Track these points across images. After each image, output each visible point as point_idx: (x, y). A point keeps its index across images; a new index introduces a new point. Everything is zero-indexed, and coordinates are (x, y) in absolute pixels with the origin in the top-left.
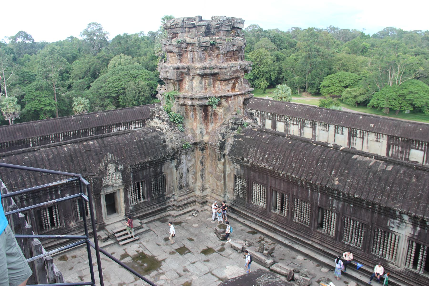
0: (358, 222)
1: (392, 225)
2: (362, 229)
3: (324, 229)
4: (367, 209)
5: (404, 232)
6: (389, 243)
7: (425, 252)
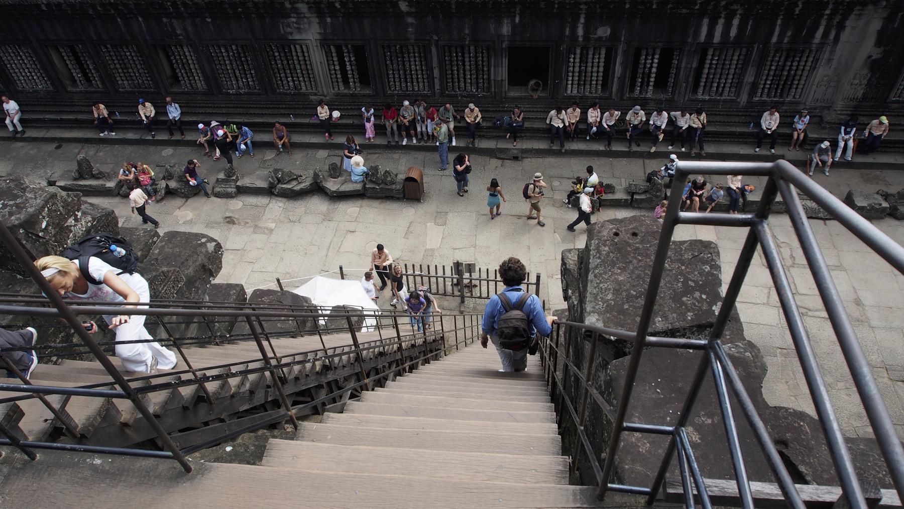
3: (182, 82)
6: (296, 62)
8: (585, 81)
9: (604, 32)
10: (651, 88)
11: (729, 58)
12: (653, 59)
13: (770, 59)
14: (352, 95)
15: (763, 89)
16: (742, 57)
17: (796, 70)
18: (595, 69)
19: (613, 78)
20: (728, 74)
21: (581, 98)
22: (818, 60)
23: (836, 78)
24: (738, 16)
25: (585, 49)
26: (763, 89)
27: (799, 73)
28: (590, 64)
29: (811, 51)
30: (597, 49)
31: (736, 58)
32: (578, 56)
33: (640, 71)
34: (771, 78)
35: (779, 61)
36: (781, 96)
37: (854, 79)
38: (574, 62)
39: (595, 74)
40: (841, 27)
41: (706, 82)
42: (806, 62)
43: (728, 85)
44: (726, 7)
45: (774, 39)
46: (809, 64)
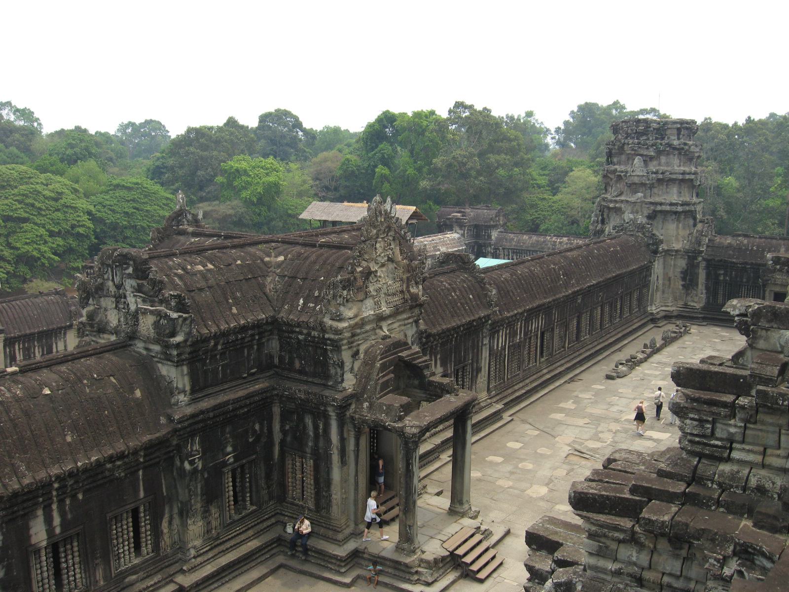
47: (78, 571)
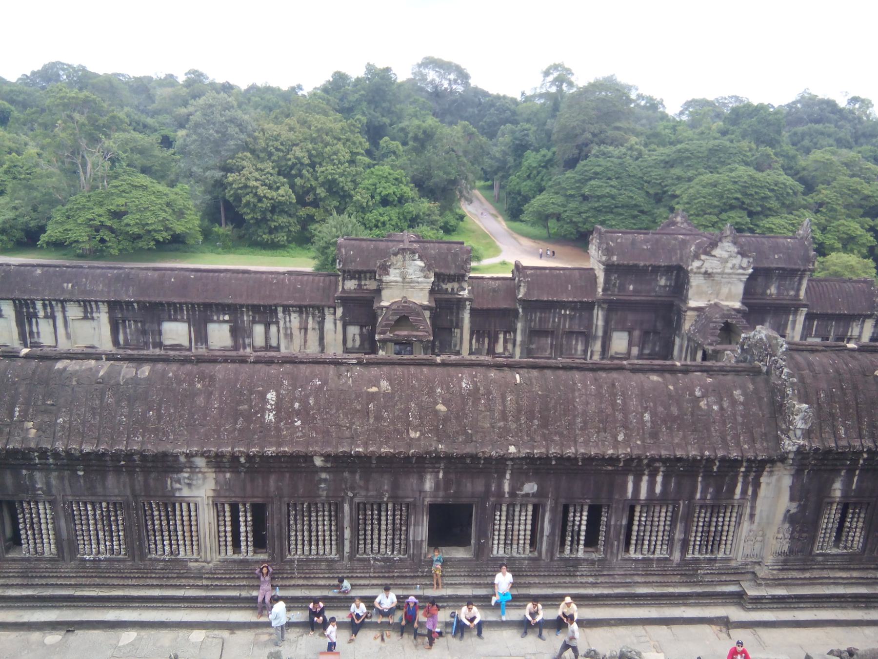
0: (104, 504)
1: (178, 486)
2: (116, 516)
4: (118, 470)
5: (200, 490)
6: (178, 522)
7: (248, 514)
8: (512, 540)
9: (530, 488)
10: (581, 547)
11: (656, 515)
12: (581, 516)
13: (696, 515)
14: (242, 562)
15: (694, 546)
16: (669, 514)
17: (723, 526)
18: (522, 527)
19: (542, 536)
20: (657, 532)
21: (509, 559)
22: (741, 515)
23: (761, 533)
24: (661, 473)
25: (511, 506)
26: (694, 546)
27: (726, 528)
28: (516, 522)
29: (733, 506)
30: (524, 506)
31: (663, 514)
32: (504, 513)
33: (569, 529)
34: (700, 534)
35: (705, 517)
36: (712, 551)
37: (778, 532)
38: (500, 520)
39: (522, 533)
40: (757, 485)
41: (637, 540)
42: (730, 517)
43: (659, 543)
44: (648, 465)
45: (698, 496)
46: (733, 519)
47: (858, 534)
